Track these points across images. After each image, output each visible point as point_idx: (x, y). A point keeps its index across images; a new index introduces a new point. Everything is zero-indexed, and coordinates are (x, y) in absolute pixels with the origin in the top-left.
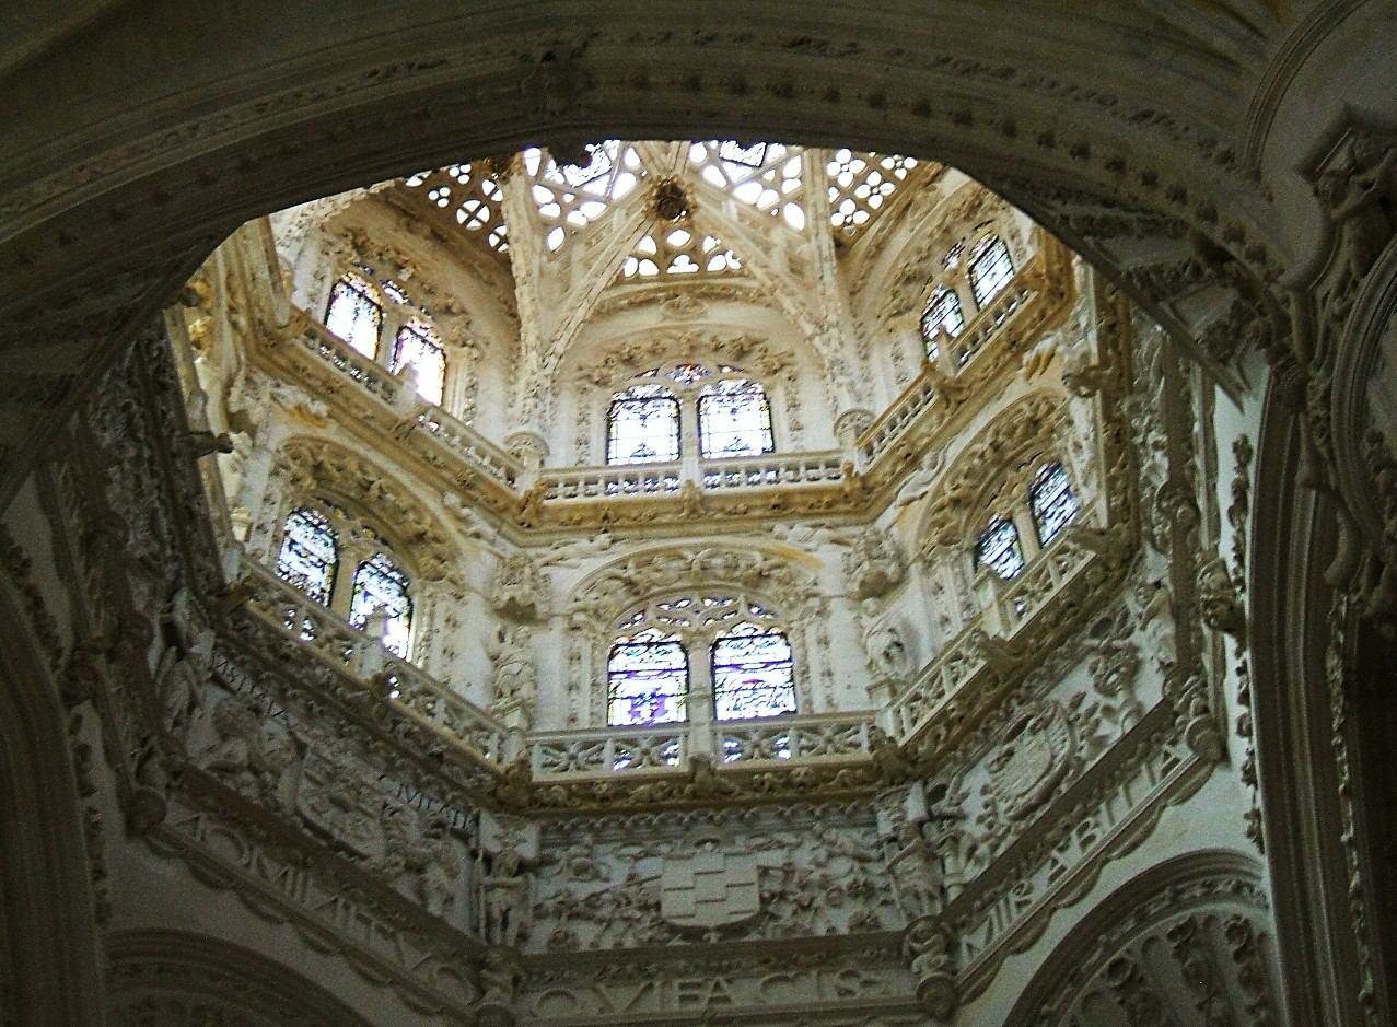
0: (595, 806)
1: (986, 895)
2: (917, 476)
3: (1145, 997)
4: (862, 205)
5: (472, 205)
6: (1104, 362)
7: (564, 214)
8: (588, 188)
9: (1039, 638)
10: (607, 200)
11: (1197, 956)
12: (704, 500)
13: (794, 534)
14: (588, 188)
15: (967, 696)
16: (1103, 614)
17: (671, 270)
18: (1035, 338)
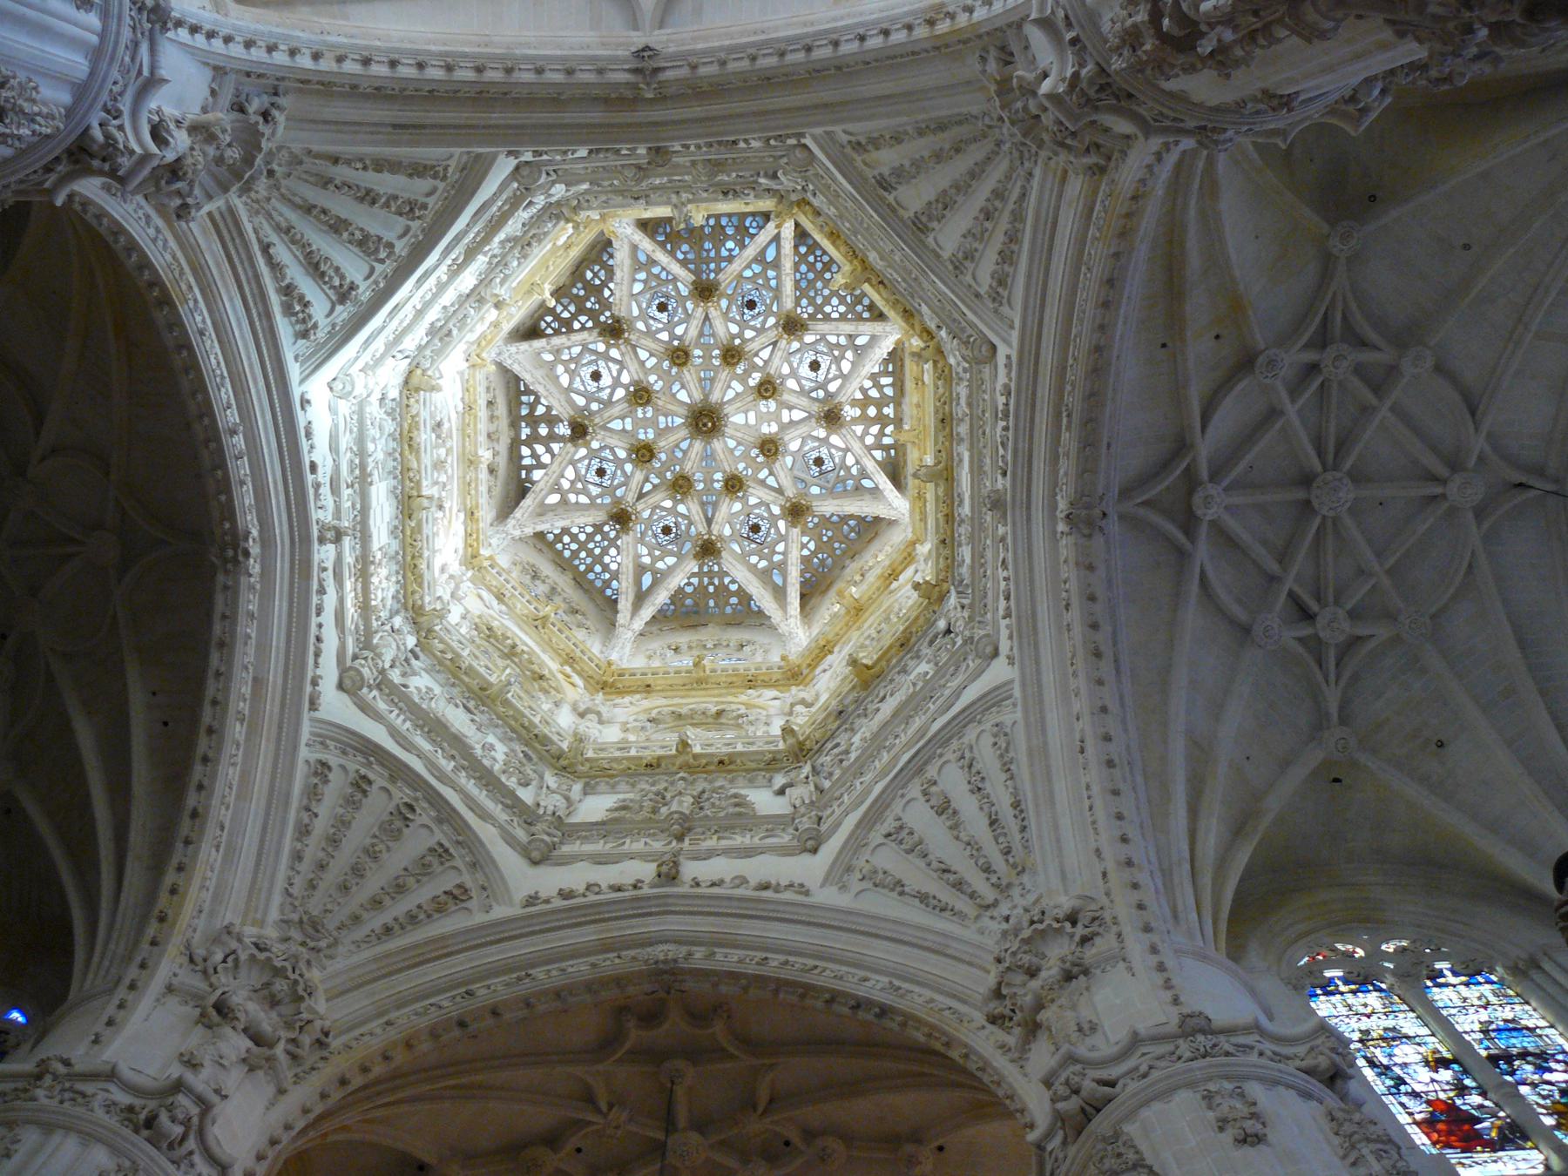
0: (405, 432)
1: (401, 704)
2: (495, 602)
3: (399, 831)
4: (558, 538)
5: (572, 308)
6: (696, 756)
7: (564, 362)
8: (578, 379)
10: (570, 389)
11: (435, 861)
12: (476, 469)
13: (458, 526)
14: (578, 379)
15: (470, 671)
16: (535, 759)
17: (523, 424)
18: (579, 674)
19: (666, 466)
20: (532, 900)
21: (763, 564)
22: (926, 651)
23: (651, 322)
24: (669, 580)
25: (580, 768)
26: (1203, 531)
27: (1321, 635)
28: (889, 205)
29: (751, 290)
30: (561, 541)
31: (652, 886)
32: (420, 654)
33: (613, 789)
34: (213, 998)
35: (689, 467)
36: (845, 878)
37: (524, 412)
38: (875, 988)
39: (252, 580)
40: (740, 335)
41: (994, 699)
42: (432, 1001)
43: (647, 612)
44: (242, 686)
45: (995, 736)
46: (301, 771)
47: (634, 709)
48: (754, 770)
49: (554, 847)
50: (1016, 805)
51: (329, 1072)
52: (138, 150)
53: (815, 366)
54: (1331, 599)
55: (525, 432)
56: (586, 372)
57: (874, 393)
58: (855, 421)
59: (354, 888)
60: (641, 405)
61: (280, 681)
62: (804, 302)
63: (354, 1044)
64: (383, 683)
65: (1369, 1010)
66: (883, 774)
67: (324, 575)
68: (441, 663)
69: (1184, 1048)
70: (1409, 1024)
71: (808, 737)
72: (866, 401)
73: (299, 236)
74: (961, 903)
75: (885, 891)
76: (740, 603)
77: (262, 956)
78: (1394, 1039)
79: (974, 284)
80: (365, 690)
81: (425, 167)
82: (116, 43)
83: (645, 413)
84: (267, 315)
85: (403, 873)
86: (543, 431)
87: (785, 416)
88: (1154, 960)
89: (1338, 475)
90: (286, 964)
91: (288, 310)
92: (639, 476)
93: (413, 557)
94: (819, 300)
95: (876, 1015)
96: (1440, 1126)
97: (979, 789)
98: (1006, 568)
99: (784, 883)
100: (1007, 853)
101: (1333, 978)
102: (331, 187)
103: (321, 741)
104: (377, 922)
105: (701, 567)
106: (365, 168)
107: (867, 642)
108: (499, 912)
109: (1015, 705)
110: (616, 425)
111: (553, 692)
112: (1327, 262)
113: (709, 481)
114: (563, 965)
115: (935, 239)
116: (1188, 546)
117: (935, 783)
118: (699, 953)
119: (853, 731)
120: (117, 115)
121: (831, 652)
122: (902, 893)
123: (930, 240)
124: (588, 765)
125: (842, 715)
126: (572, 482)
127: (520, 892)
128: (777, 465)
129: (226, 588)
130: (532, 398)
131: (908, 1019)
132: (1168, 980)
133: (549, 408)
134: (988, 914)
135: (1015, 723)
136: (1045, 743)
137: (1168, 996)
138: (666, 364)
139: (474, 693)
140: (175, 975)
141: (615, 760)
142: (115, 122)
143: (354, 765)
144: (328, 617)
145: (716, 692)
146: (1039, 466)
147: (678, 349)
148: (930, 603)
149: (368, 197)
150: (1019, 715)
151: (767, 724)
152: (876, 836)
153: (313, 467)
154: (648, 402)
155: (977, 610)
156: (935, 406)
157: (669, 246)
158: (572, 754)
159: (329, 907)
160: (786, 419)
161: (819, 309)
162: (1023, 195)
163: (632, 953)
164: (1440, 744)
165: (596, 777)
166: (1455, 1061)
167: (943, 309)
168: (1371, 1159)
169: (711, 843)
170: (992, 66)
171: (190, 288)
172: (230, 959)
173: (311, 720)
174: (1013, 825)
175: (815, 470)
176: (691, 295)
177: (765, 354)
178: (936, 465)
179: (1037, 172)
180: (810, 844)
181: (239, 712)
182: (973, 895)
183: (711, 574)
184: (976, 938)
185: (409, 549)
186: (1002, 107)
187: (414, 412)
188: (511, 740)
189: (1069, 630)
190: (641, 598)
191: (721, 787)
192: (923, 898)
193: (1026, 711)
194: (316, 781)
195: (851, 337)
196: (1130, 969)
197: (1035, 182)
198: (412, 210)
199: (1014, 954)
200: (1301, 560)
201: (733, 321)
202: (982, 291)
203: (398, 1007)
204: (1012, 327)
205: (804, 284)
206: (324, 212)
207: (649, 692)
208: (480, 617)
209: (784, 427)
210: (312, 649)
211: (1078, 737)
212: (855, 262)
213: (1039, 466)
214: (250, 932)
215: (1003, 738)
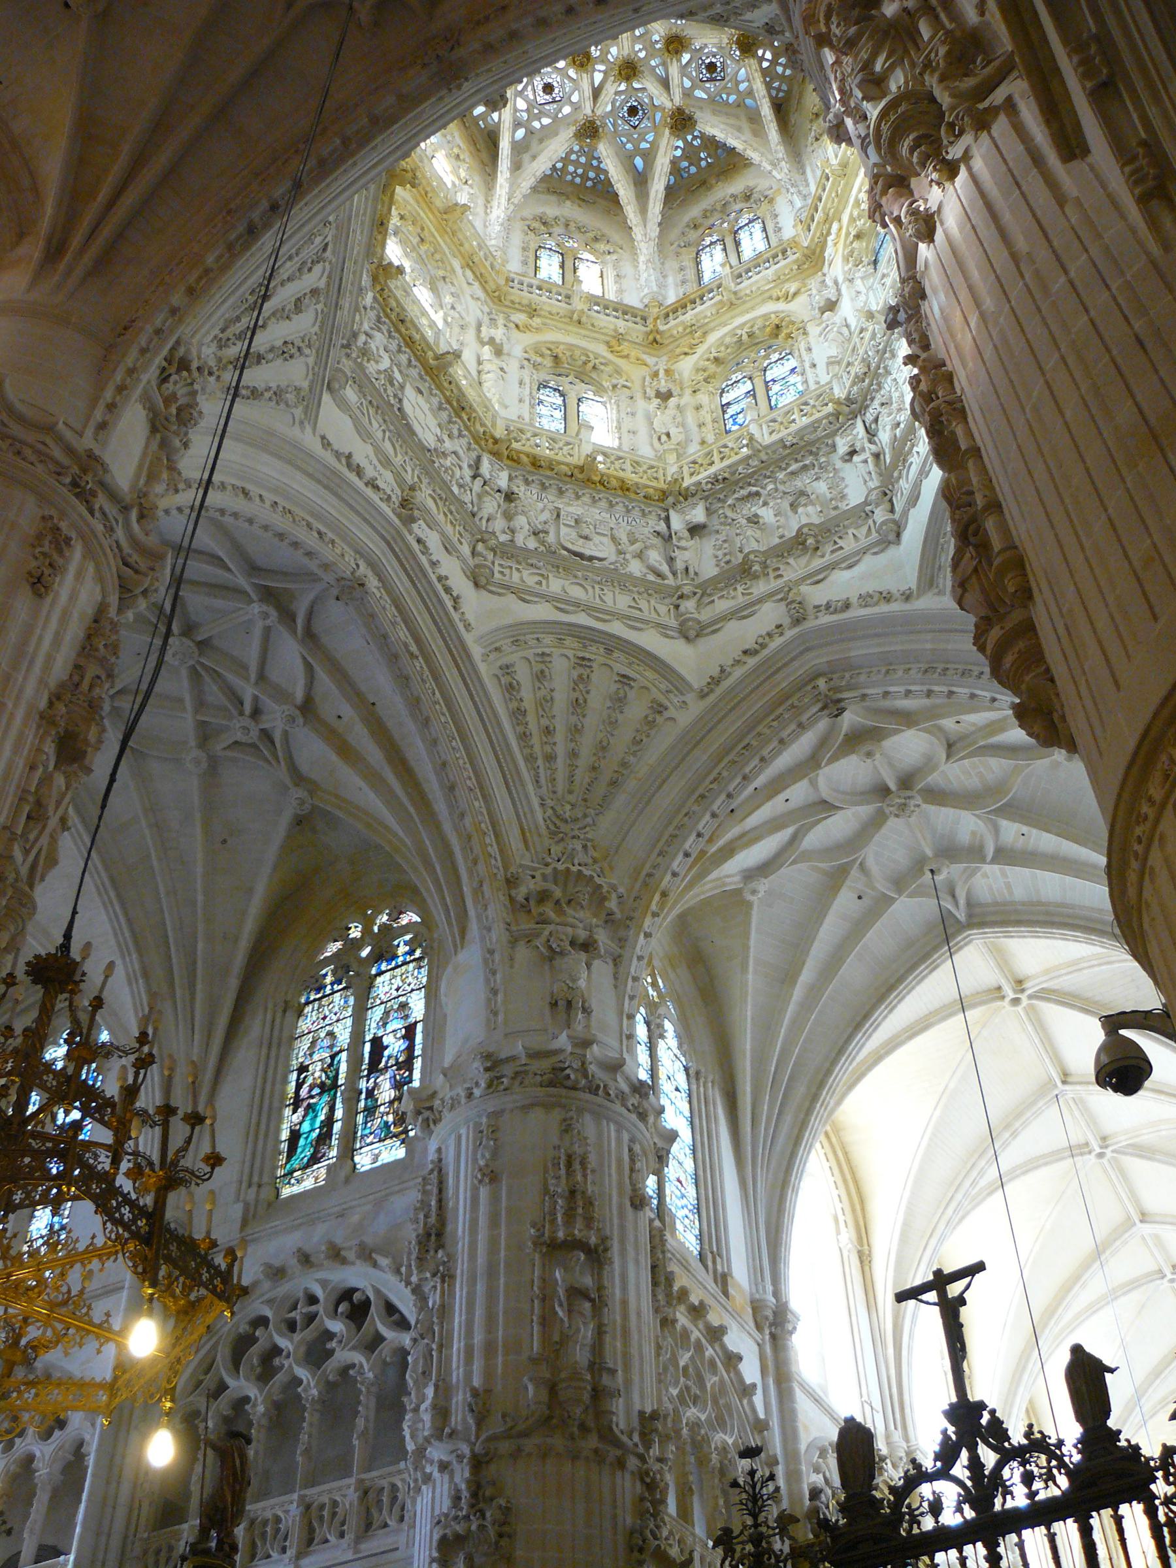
112: (299, 778)
146: (401, 583)
170: (612, 904)
195: (530, 132)
197: (535, 802)
213: (401, 583)
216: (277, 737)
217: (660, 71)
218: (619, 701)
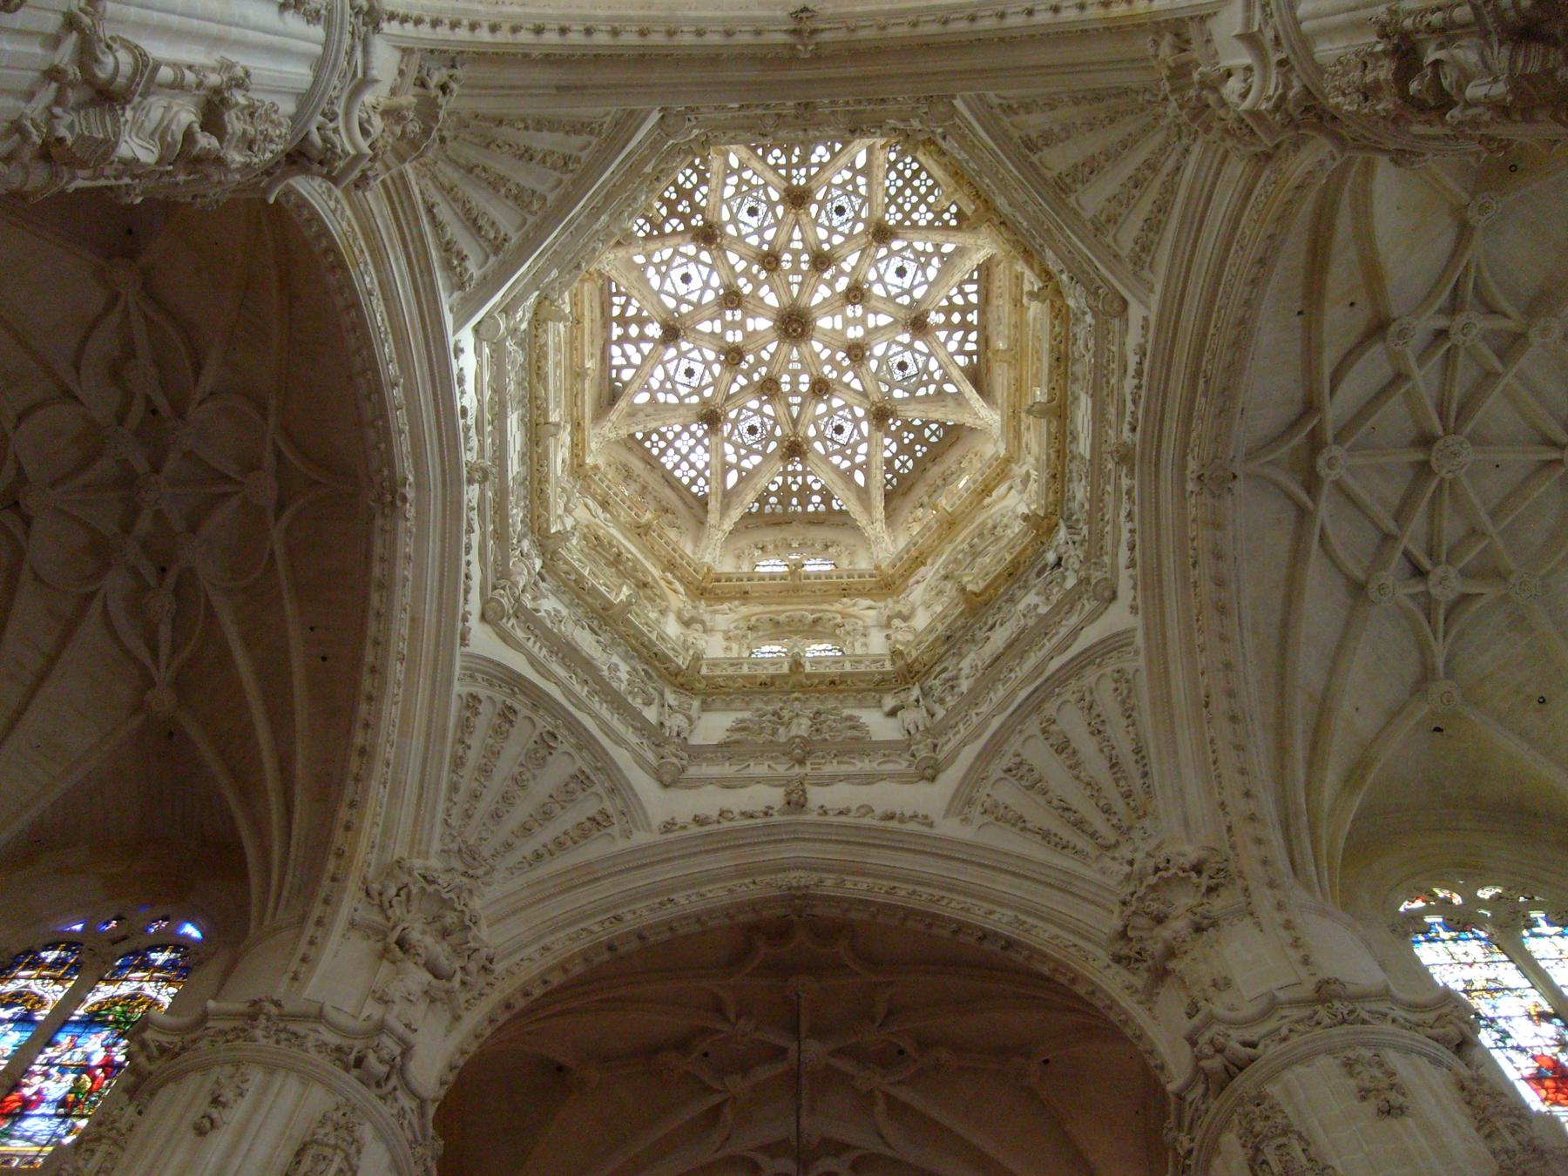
1: (537, 632)
2: (600, 511)
3: (544, 758)
6: (808, 676)
9: (634, 635)
10: (661, 291)
14: (668, 280)
17: (614, 325)
18: (680, 580)
19: (754, 368)
20: (668, 827)
21: (846, 464)
22: (1033, 580)
23: (741, 226)
24: (756, 480)
25: (698, 685)
26: (1326, 489)
27: (1433, 591)
28: (1032, 164)
29: (839, 196)
30: (649, 439)
31: (781, 812)
32: (547, 576)
33: (728, 707)
34: (394, 936)
35: (776, 370)
36: (966, 810)
37: (616, 311)
38: (1001, 921)
39: (408, 524)
40: (828, 240)
41: (1114, 644)
42: (583, 925)
43: (735, 514)
44: (401, 626)
45: (1116, 681)
46: (455, 705)
47: (732, 616)
48: (864, 690)
49: (683, 769)
50: (1137, 751)
51: (494, 998)
52: (352, 152)
53: (901, 272)
54: (1444, 557)
55: (617, 331)
56: (676, 275)
57: (959, 300)
58: (939, 327)
59: (506, 817)
60: (730, 309)
61: (434, 620)
62: (893, 209)
63: (515, 969)
64: (520, 612)
65: (1470, 960)
66: (1001, 707)
67: (471, 514)
68: (565, 584)
69: (1322, 1012)
70: (1509, 974)
71: (916, 660)
72: (950, 309)
73: (460, 194)
74: (1081, 842)
75: (1007, 826)
76: (822, 502)
77: (431, 889)
78: (1497, 990)
79: (1113, 244)
80: (505, 620)
81: (583, 124)
82: (338, 51)
83: (733, 315)
84: (429, 271)
85: (548, 800)
86: (634, 331)
87: (872, 321)
88: (1279, 918)
89: (1461, 438)
90: (452, 895)
91: (447, 266)
92: (727, 377)
93: (540, 482)
94: (907, 207)
95: (1002, 948)
96: (1548, 1083)
97: (1099, 732)
98: (1131, 520)
99: (908, 813)
100: (1127, 797)
101: (1434, 924)
102: (493, 146)
103: (470, 673)
104: (527, 848)
105: (785, 468)
106: (526, 128)
107: (960, 556)
108: (641, 838)
109: (1136, 653)
110: (705, 327)
111: (658, 600)
112: (1464, 232)
113: (795, 383)
114: (703, 890)
115: (1077, 201)
116: (1310, 504)
117: (1054, 722)
118: (830, 880)
119: (961, 656)
120: (333, 117)
121: (923, 564)
122: (1023, 829)
123: (1072, 200)
124: (704, 682)
125: (951, 640)
126: (662, 383)
127: (658, 817)
128: (863, 369)
129: (383, 530)
130: (623, 299)
131: (1034, 952)
132: (1297, 939)
133: (640, 310)
134: (1110, 854)
135: (1137, 671)
136: (1169, 693)
137: (1295, 955)
138: (755, 268)
139: (596, 612)
140: (356, 910)
141: (730, 678)
142: (331, 125)
143: (500, 696)
144: (474, 556)
145: (809, 599)
146: (1172, 426)
147: (768, 254)
148: (1037, 535)
149: (527, 155)
150: (1141, 662)
151: (865, 635)
152: (996, 769)
153: (464, 412)
154: (738, 306)
155: (1094, 551)
156: (1051, 345)
157: (760, 152)
158: (690, 671)
159: (484, 835)
160: (871, 324)
161: (907, 216)
162: (1178, 169)
163: (767, 878)
164: (1542, 701)
165: (713, 694)
166: (1556, 1015)
167: (1073, 259)
168: (1506, 1134)
169: (831, 768)
170: (1165, 49)
171: (362, 251)
172: (402, 893)
173: (462, 655)
174: (1134, 771)
175: (898, 375)
176: (782, 201)
177: (853, 259)
178: (1049, 402)
179: (1196, 151)
180: (929, 772)
181: (399, 653)
182: (1093, 835)
183: (794, 474)
184: (1098, 877)
185: (536, 475)
186: (1173, 91)
187: (542, 341)
188: (632, 658)
189: (1196, 587)
190: (728, 497)
191: (835, 708)
192: (1045, 835)
193: (1149, 661)
194: (468, 714)
196: (1258, 924)
198: (566, 164)
199: (1141, 899)
200: (1418, 522)
201: (822, 226)
202: (1123, 254)
203: (552, 932)
204: (1151, 290)
205: (893, 191)
206: (485, 170)
207: (746, 599)
208: (587, 527)
209: (868, 332)
210: (462, 587)
211: (1202, 692)
212: (978, 202)
213: (1172, 426)
214: (418, 862)
215: (1124, 685)
216: (1443, 298)
217: (797, 234)
218: (1048, 139)
